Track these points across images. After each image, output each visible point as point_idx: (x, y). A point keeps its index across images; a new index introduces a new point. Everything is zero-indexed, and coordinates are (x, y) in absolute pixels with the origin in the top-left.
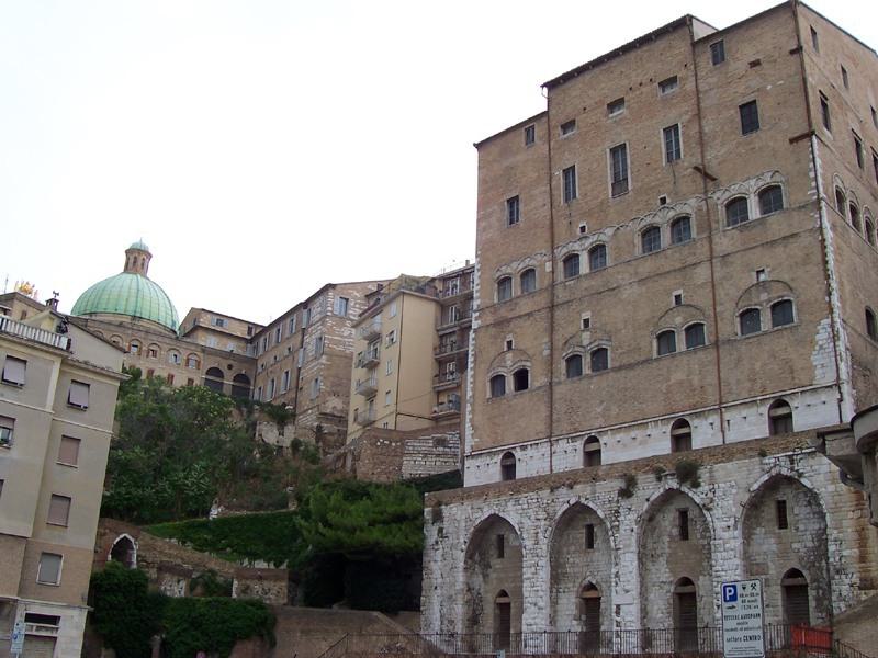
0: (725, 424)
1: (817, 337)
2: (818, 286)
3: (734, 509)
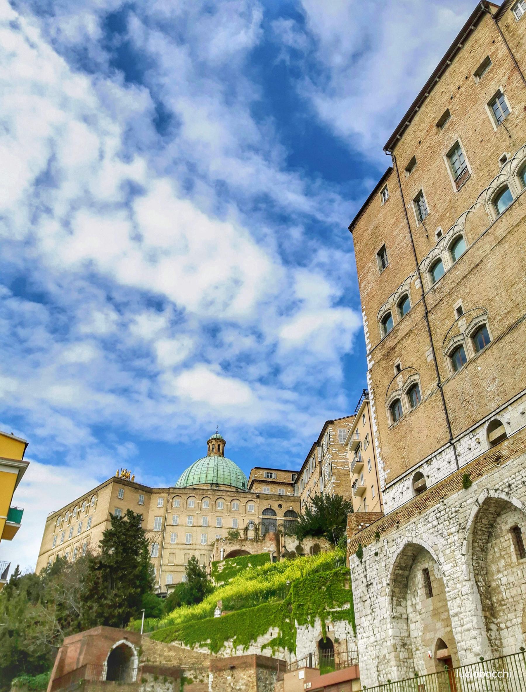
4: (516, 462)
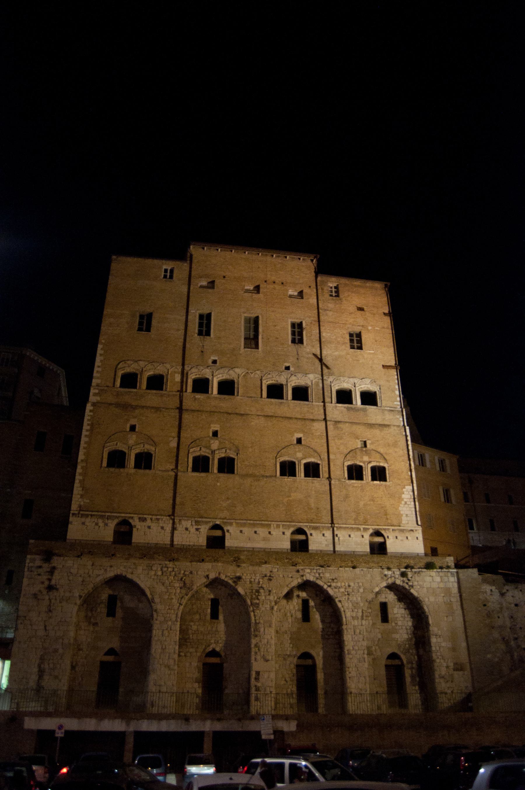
0: (336, 538)
1: (403, 496)
2: (403, 463)
3: (362, 604)
4: (251, 568)
